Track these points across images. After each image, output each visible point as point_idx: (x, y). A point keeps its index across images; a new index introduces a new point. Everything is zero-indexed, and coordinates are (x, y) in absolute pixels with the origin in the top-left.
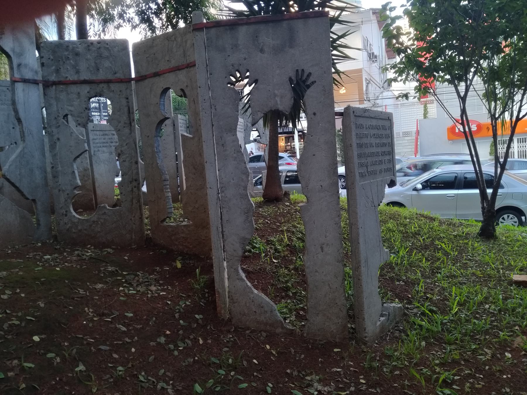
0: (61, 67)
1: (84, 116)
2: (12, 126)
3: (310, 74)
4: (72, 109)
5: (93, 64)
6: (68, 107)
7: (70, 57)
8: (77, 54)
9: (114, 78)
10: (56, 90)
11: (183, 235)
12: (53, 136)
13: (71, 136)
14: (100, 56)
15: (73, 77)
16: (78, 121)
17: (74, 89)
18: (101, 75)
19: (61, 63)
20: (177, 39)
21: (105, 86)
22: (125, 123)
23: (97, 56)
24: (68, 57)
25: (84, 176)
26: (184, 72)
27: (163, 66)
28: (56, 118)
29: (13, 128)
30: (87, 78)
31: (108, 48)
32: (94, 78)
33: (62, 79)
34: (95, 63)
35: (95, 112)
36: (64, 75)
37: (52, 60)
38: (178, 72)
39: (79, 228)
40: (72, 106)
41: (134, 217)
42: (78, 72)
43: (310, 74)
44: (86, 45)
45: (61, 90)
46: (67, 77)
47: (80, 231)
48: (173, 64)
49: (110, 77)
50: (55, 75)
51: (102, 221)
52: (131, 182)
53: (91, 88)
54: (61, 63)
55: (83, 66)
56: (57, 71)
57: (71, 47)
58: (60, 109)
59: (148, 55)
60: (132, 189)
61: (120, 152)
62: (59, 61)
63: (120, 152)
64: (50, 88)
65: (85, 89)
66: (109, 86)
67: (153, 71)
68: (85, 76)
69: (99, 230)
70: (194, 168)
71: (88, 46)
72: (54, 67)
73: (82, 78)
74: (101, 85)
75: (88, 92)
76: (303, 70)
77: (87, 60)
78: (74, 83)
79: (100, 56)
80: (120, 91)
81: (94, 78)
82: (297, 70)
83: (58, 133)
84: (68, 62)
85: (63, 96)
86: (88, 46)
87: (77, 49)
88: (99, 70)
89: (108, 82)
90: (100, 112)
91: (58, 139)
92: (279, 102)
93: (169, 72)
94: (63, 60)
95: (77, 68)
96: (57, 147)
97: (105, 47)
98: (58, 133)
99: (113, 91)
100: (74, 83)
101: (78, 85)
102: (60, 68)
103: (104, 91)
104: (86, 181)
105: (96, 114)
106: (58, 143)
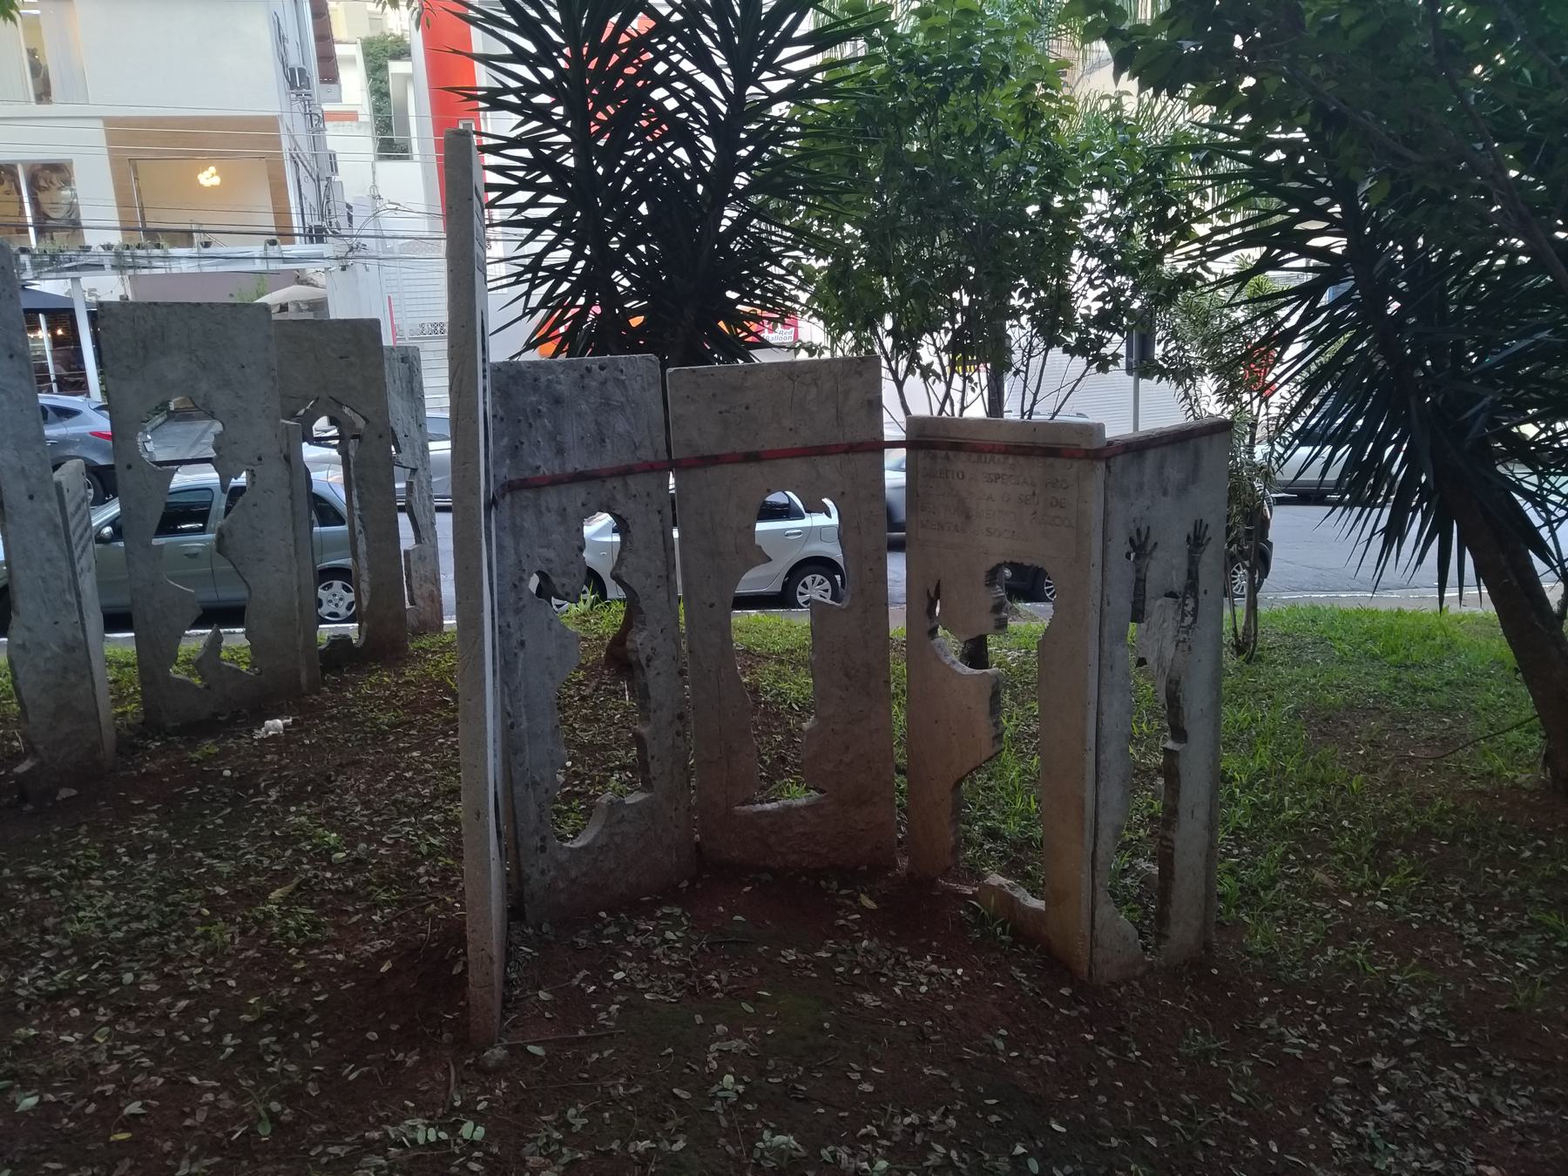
0: (524, 439)
1: (576, 572)
4: (551, 554)
5: (592, 427)
6: (541, 550)
8: (558, 401)
9: (636, 462)
11: (802, 830)
12: (509, 636)
14: (606, 403)
15: (545, 463)
17: (551, 498)
18: (608, 459)
19: (524, 426)
20: (819, 382)
21: (617, 483)
22: (660, 577)
25: (65, 669)
26: (835, 460)
27: (767, 441)
28: (515, 586)
30: (581, 468)
31: (623, 382)
32: (594, 465)
33: (527, 474)
34: (597, 423)
36: (530, 460)
37: (502, 419)
38: (818, 458)
39: (573, 874)
40: (548, 546)
42: (560, 451)
44: (576, 375)
45: (525, 503)
46: (538, 468)
47: (573, 881)
48: (805, 437)
49: (626, 459)
50: (508, 462)
54: (524, 426)
56: (515, 451)
58: (524, 559)
59: (724, 408)
62: (519, 421)
66: (626, 484)
67: (741, 448)
68: (574, 463)
69: (613, 866)
70: (847, 675)
71: (582, 376)
72: (506, 440)
73: (569, 469)
74: (609, 484)
75: (583, 505)
77: (579, 415)
78: (556, 481)
79: (606, 403)
80: (648, 495)
83: (521, 627)
85: (528, 521)
87: (559, 387)
88: (604, 441)
89: (624, 472)
91: (522, 644)
93: (793, 457)
94: (527, 418)
95: (559, 438)
97: (617, 380)
98: (521, 627)
100: (556, 481)
101: (562, 487)
106: (521, 655)
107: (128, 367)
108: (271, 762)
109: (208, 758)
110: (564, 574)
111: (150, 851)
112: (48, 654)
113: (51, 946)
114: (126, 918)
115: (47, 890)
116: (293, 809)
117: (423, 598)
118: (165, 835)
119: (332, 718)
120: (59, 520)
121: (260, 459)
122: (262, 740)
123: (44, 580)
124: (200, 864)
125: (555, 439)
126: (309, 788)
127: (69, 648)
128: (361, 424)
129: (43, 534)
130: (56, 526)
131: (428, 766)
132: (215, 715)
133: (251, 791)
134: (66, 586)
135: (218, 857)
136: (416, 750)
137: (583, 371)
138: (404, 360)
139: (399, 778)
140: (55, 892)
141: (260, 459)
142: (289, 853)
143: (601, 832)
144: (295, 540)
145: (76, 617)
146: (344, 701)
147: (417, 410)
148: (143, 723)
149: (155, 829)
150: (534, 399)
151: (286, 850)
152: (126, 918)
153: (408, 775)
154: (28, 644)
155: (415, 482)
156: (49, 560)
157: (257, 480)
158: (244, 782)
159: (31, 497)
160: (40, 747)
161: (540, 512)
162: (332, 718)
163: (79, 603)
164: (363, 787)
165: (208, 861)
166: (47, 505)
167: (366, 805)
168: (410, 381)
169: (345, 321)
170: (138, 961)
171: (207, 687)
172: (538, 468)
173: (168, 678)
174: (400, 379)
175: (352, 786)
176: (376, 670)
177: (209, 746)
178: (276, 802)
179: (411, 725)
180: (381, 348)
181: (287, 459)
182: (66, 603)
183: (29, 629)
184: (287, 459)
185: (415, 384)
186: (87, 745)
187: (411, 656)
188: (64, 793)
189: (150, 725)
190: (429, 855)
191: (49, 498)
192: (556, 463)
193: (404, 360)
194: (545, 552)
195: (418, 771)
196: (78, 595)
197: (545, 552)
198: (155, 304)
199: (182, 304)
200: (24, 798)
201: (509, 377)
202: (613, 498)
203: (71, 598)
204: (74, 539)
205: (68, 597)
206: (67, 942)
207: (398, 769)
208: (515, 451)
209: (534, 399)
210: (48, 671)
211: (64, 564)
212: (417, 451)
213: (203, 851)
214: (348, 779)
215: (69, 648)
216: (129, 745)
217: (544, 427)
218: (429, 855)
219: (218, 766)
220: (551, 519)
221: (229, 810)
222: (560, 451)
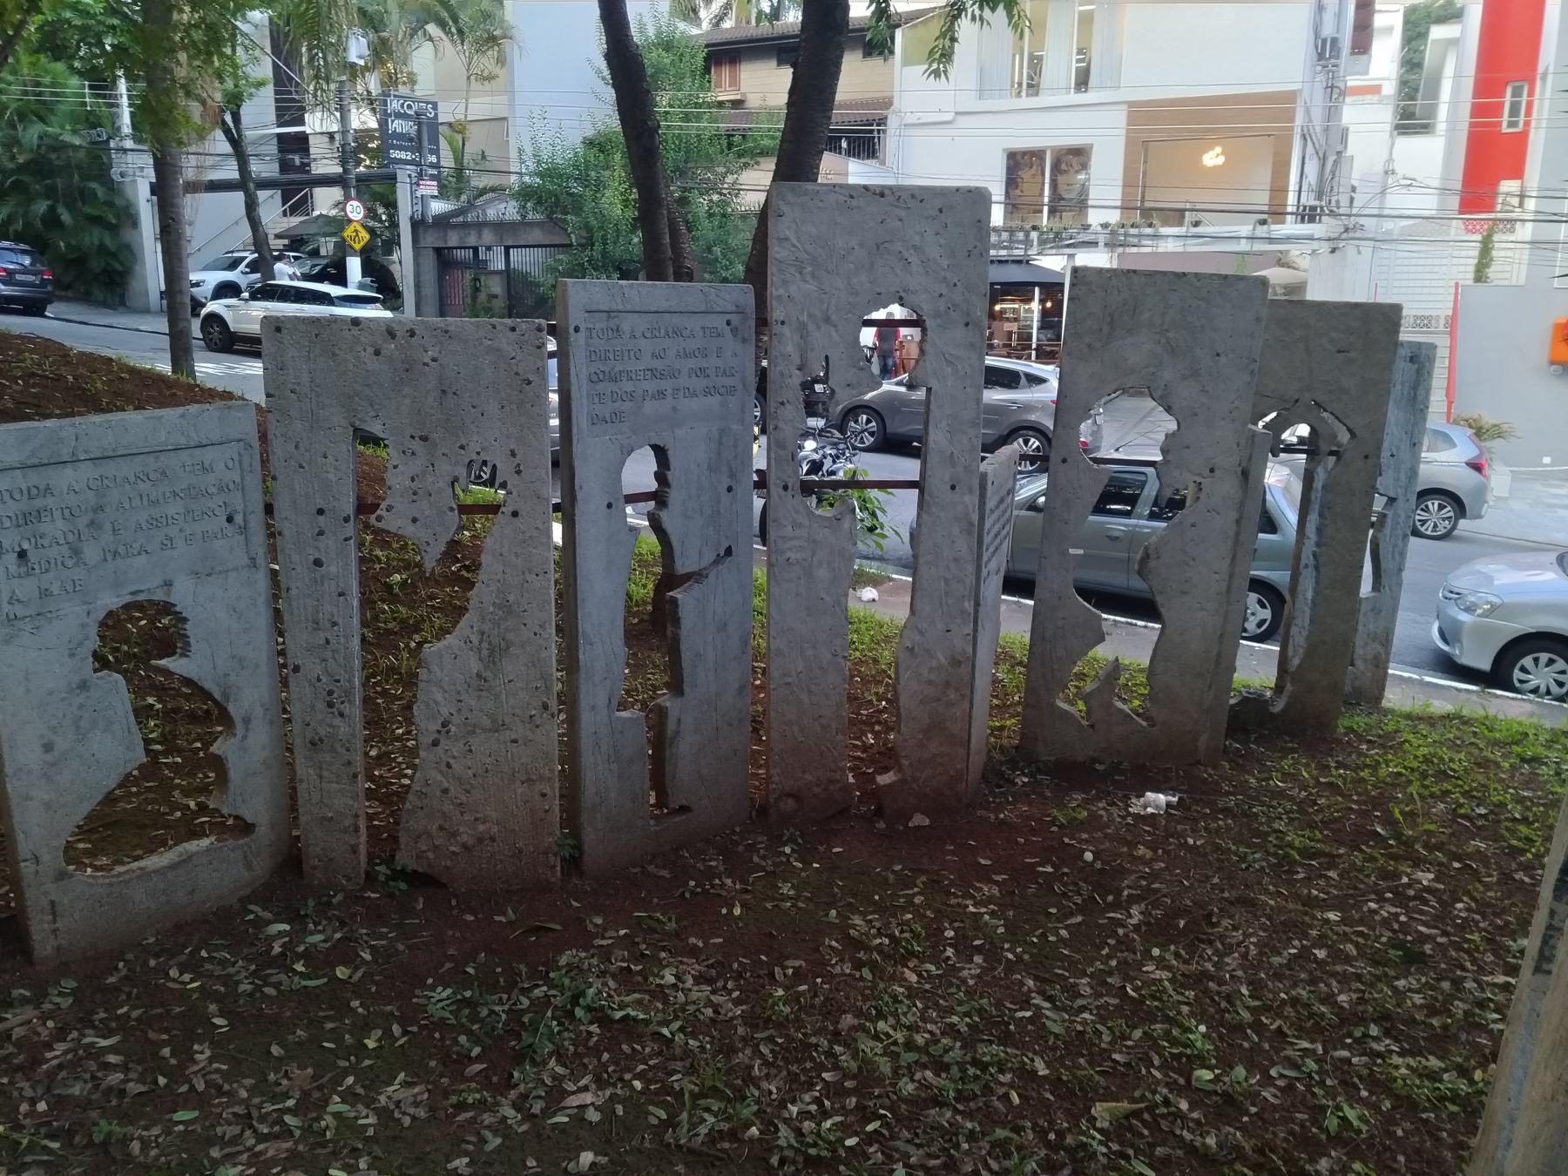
2: (726, 482)
25: (947, 684)
29: (730, 489)
35: (401, 148)
90: (419, 149)
104: (950, 704)
105: (402, 155)
107: (1089, 345)
108: (1141, 859)
109: (1074, 826)
111: (979, 950)
112: (934, 663)
113: (836, 1067)
114: (925, 1059)
115: (858, 965)
116: (1156, 952)
117: (1365, 661)
118: (1001, 930)
119: (1226, 811)
120: (975, 517)
121: (1212, 470)
122: (1137, 817)
123: (947, 581)
124: (1026, 1003)
126: (1182, 923)
127: (956, 662)
128: (1344, 437)
129: (956, 530)
130: (971, 524)
131: (1351, 949)
132: (1094, 760)
133: (1110, 898)
134: (967, 593)
135: (1049, 999)
136: (1332, 908)
138: (1412, 359)
139: (1305, 954)
140: (867, 973)
141: (1212, 470)
142: (1137, 1034)
144: (1231, 576)
145: (969, 629)
146: (1243, 788)
147: (1415, 424)
148: (1017, 748)
149: (993, 914)
151: (1134, 1027)
152: (925, 1059)
153: (1321, 954)
154: (916, 649)
155: (1390, 513)
156: (956, 560)
157: (1202, 495)
158: (1104, 879)
159: (953, 487)
160: (905, 762)
162: (1226, 811)
163: (976, 612)
164: (1253, 951)
165: (1038, 1000)
166: (967, 498)
167: (1257, 987)
168: (1415, 386)
169: (1357, 305)
170: (919, 1146)
171: (1092, 726)
173: (1053, 706)
174: (1403, 384)
175: (1239, 944)
176: (1293, 750)
177: (1076, 805)
178: (1137, 928)
179: (1332, 861)
180: (1397, 344)
181: (1245, 474)
182: (963, 612)
183: (921, 633)
184: (1245, 474)
185: (1421, 392)
186: (952, 773)
187: (1339, 742)
188: (920, 820)
189: (1022, 755)
190: (1337, 1140)
191: (971, 491)
193: (1412, 359)
195: (1337, 955)
196: (977, 604)
198: (1135, 271)
199: (1164, 273)
200: (879, 812)
203: (969, 606)
204: (987, 539)
205: (967, 604)
206: (854, 1065)
207: (1306, 936)
210: (930, 682)
211: (970, 568)
212: (1402, 476)
213: (1036, 978)
214: (1235, 928)
215: (956, 662)
216: (995, 775)
218: (1337, 1140)
219: (1081, 841)
221: (1079, 919)
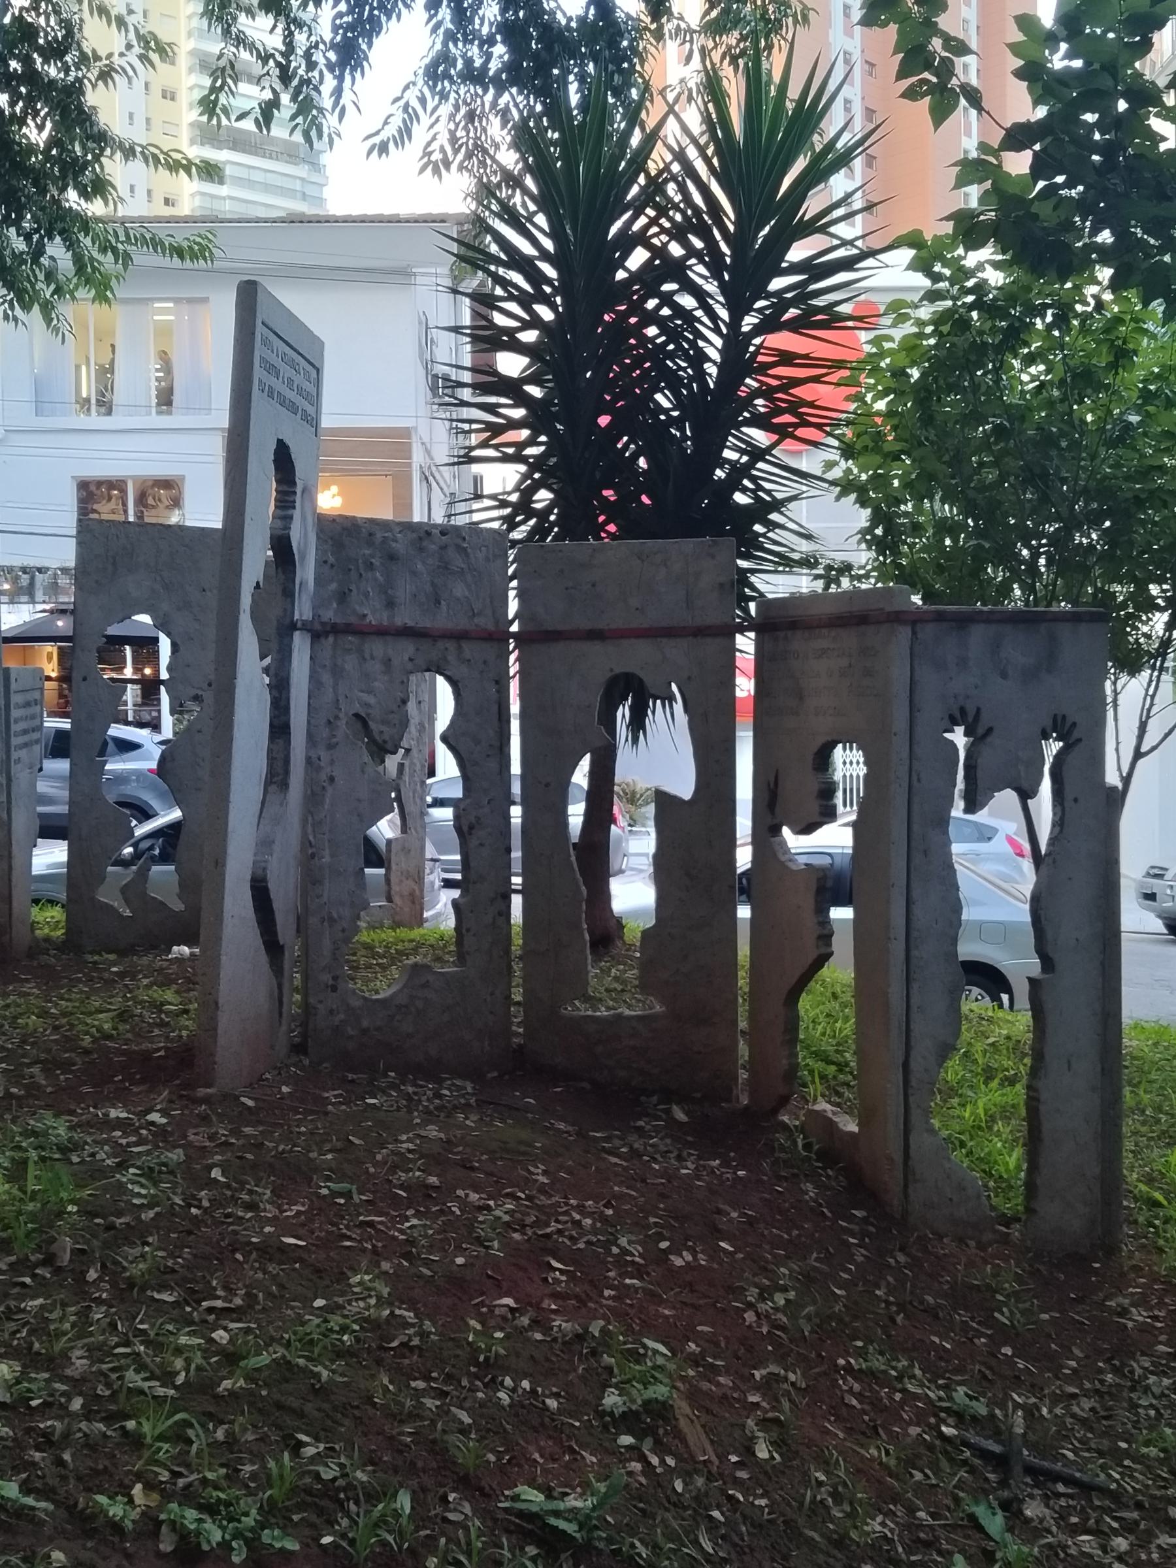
0: (353, 587)
3: (1074, 724)
4: (371, 700)
7: (376, 562)
8: (392, 557)
10: (335, 646)
13: (363, 772)
15: (373, 613)
16: (382, 732)
17: (377, 647)
18: (442, 620)
19: (354, 574)
21: (451, 645)
23: (439, 567)
24: (371, 563)
28: (329, 722)
30: (410, 623)
32: (425, 623)
33: (353, 619)
34: (433, 584)
36: (357, 608)
40: (369, 692)
41: (492, 994)
42: (390, 604)
43: (1074, 724)
44: (415, 535)
45: (347, 646)
46: (365, 616)
50: (335, 605)
51: (420, 1004)
52: (492, 901)
53: (418, 649)
54: (354, 574)
55: (404, 589)
56: (343, 597)
57: (379, 536)
60: (494, 918)
61: (473, 820)
62: (350, 570)
63: (473, 820)
64: (323, 640)
65: (405, 650)
66: (460, 648)
68: (405, 617)
71: (420, 539)
73: (399, 622)
74: (441, 644)
75: (411, 660)
76: (1064, 717)
78: (382, 632)
81: (428, 626)
82: (1055, 716)
83: (332, 762)
84: (370, 574)
85: (350, 663)
86: (420, 539)
87: (394, 545)
89: (460, 636)
91: (332, 779)
92: (1022, 774)
94: (358, 569)
95: (390, 592)
96: (328, 801)
98: (332, 762)
99: (469, 661)
100: (382, 632)
101: (389, 638)
102: (351, 591)
103: (449, 658)
106: (330, 790)
110: (384, 722)
125: (386, 593)
137: (422, 534)
143: (401, 991)
150: (367, 552)
161: (364, 659)
172: (365, 616)
192: (385, 615)
194: (365, 697)
197: (365, 697)
201: (344, 529)
202: (445, 659)
208: (343, 597)
209: (367, 552)
217: (376, 580)
220: (376, 667)
222: (390, 604)
